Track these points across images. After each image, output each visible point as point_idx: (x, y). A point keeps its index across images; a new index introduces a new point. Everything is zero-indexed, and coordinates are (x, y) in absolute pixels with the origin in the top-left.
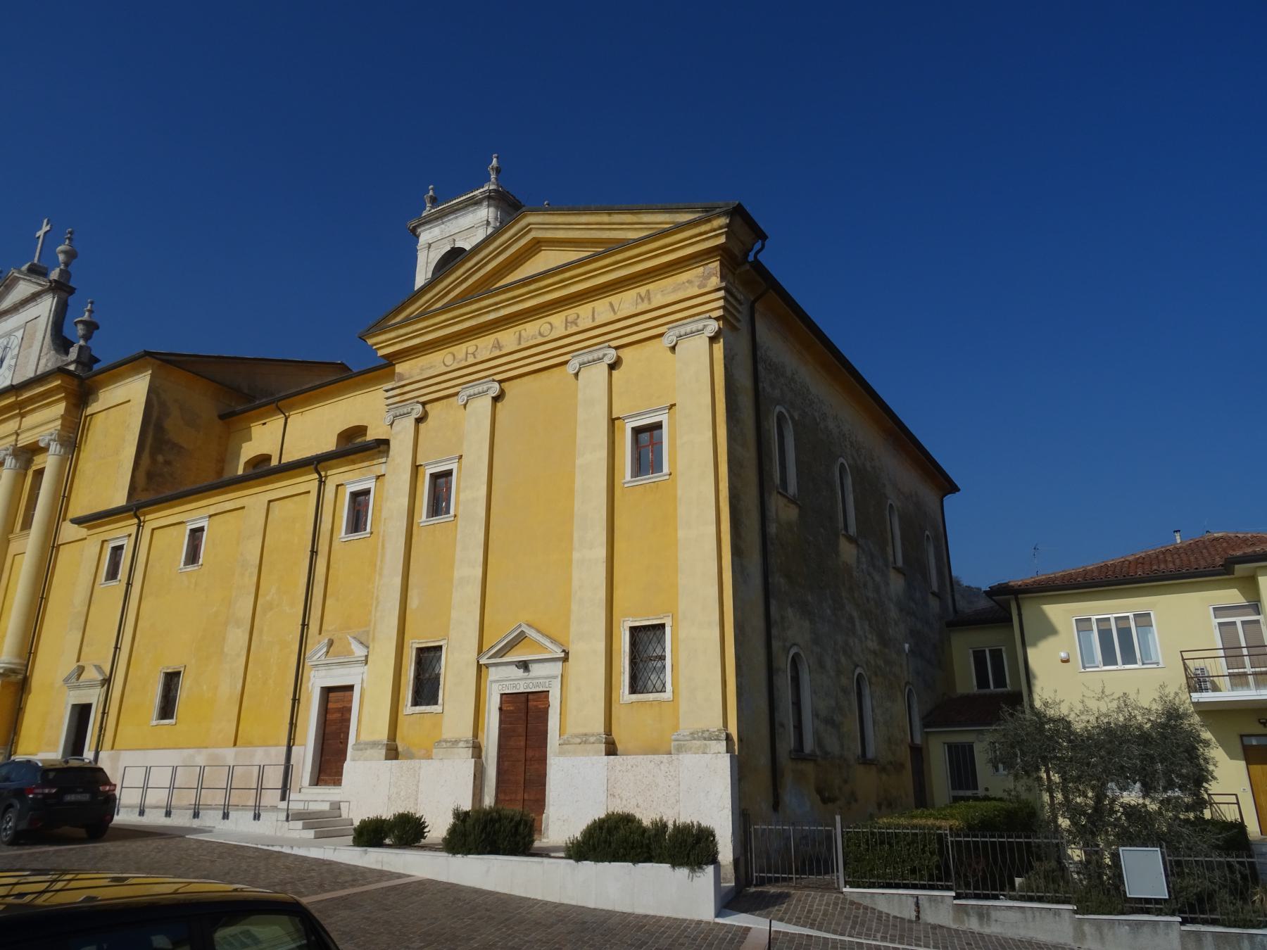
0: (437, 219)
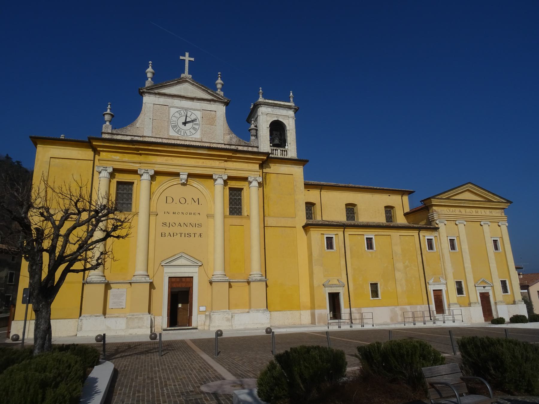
0: (271, 106)
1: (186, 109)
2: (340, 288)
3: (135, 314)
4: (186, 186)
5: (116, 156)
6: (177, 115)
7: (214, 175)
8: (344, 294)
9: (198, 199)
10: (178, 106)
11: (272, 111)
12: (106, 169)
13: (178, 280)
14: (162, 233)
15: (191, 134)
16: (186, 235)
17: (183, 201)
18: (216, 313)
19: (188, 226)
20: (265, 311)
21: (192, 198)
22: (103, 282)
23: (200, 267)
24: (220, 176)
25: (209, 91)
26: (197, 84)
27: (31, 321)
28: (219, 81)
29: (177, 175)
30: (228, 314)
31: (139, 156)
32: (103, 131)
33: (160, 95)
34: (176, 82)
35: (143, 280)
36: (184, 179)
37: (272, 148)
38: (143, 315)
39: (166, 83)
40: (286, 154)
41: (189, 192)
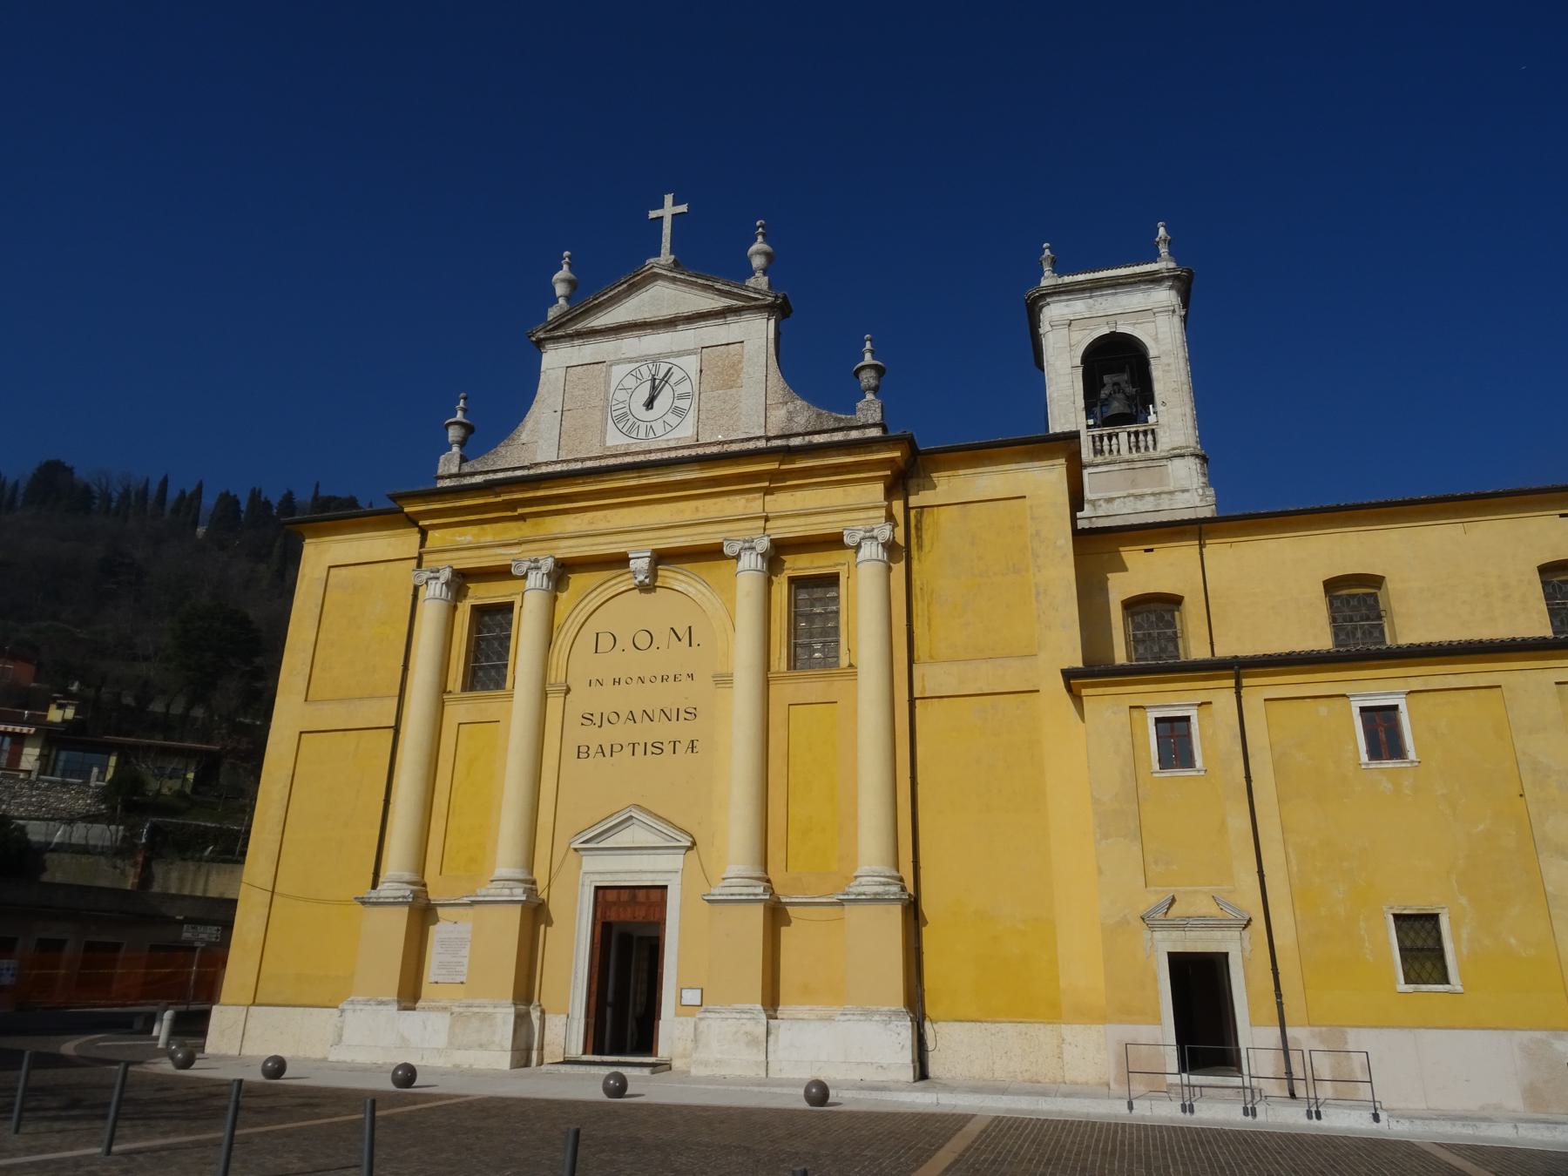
0: (1083, 290)
1: (655, 359)
2: (1228, 933)
3: (477, 1002)
4: (655, 592)
5: (465, 535)
6: (630, 382)
7: (726, 543)
8: (1246, 962)
9: (690, 628)
10: (633, 356)
11: (1090, 308)
12: (438, 575)
13: (625, 896)
14: (579, 747)
15: (668, 428)
16: (650, 748)
17: (643, 640)
18: (713, 1015)
19: (656, 719)
20: (893, 1018)
21: (672, 629)
22: (401, 900)
23: (690, 853)
24: (747, 545)
25: (718, 286)
26: (682, 277)
27: (252, 1009)
28: (759, 245)
29: (620, 561)
30: (754, 1019)
31: (520, 524)
32: (440, 471)
33: (583, 339)
34: (625, 285)
35: (505, 894)
36: (640, 572)
37: (1097, 432)
38: (495, 1007)
39: (597, 299)
40: (1150, 443)
41: (657, 610)
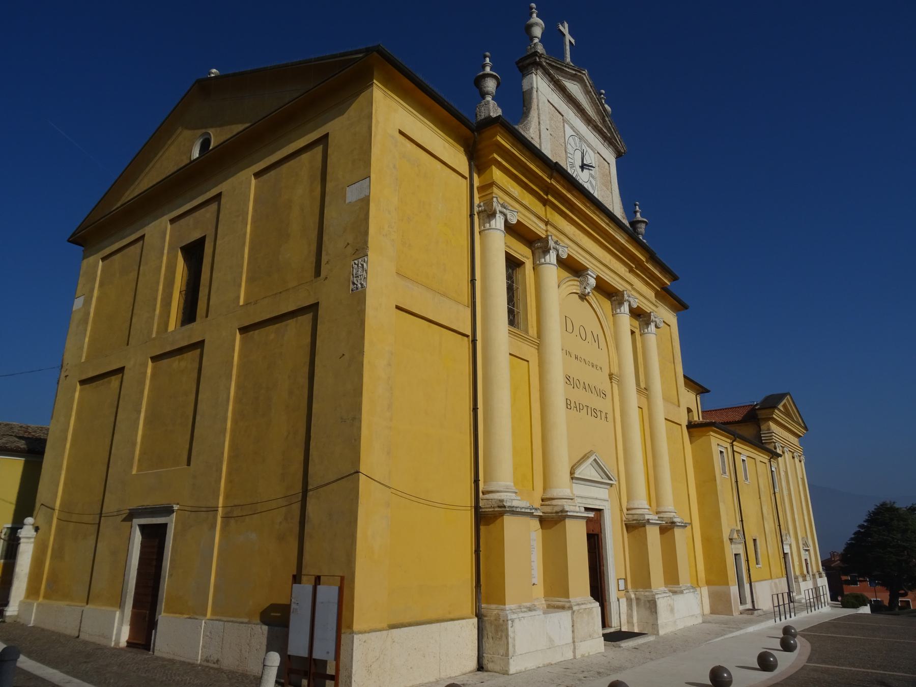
34: (574, 72)
